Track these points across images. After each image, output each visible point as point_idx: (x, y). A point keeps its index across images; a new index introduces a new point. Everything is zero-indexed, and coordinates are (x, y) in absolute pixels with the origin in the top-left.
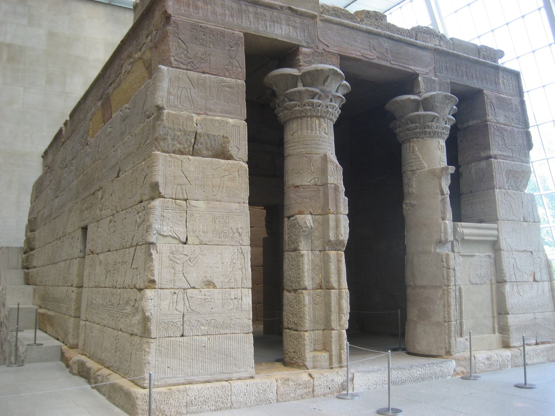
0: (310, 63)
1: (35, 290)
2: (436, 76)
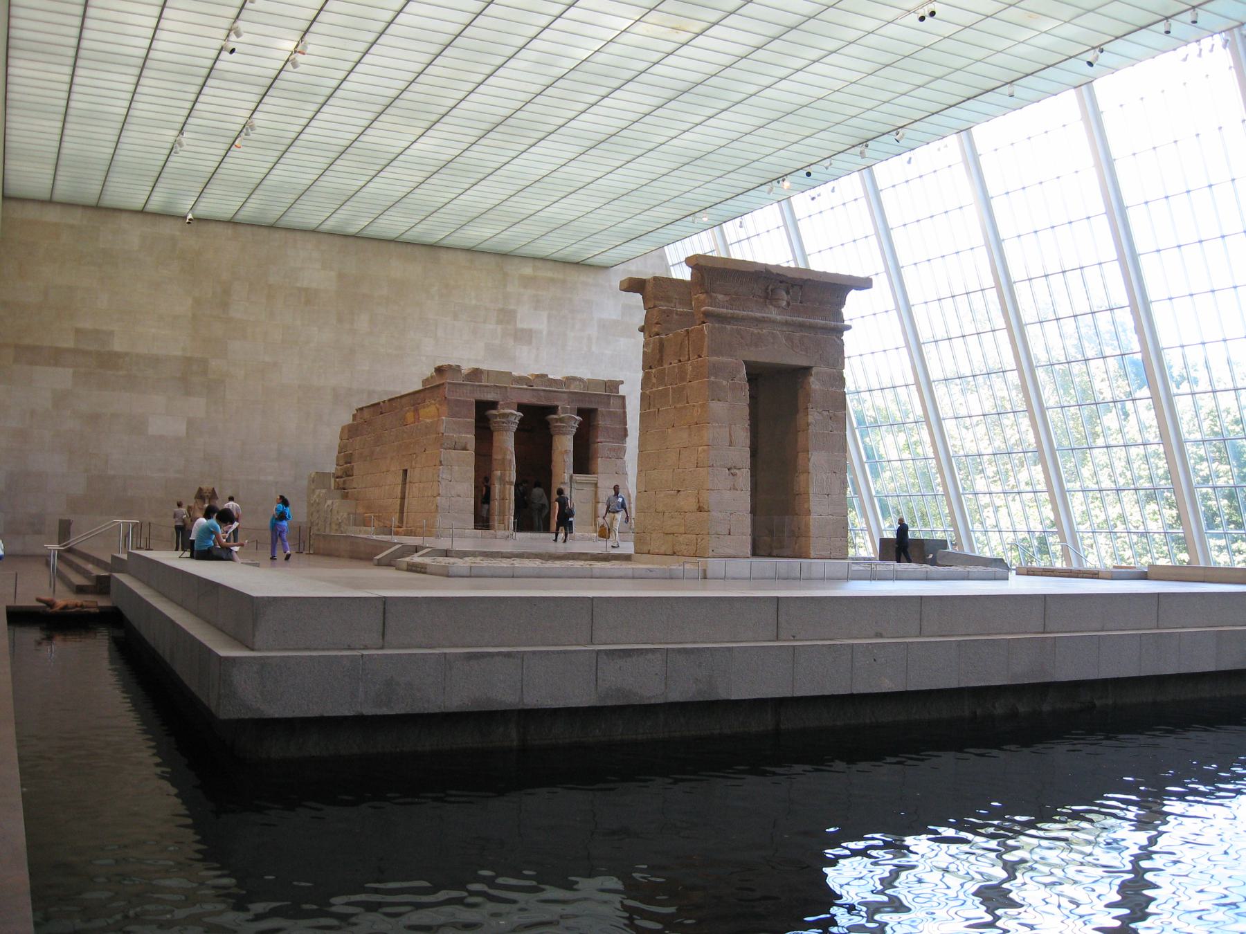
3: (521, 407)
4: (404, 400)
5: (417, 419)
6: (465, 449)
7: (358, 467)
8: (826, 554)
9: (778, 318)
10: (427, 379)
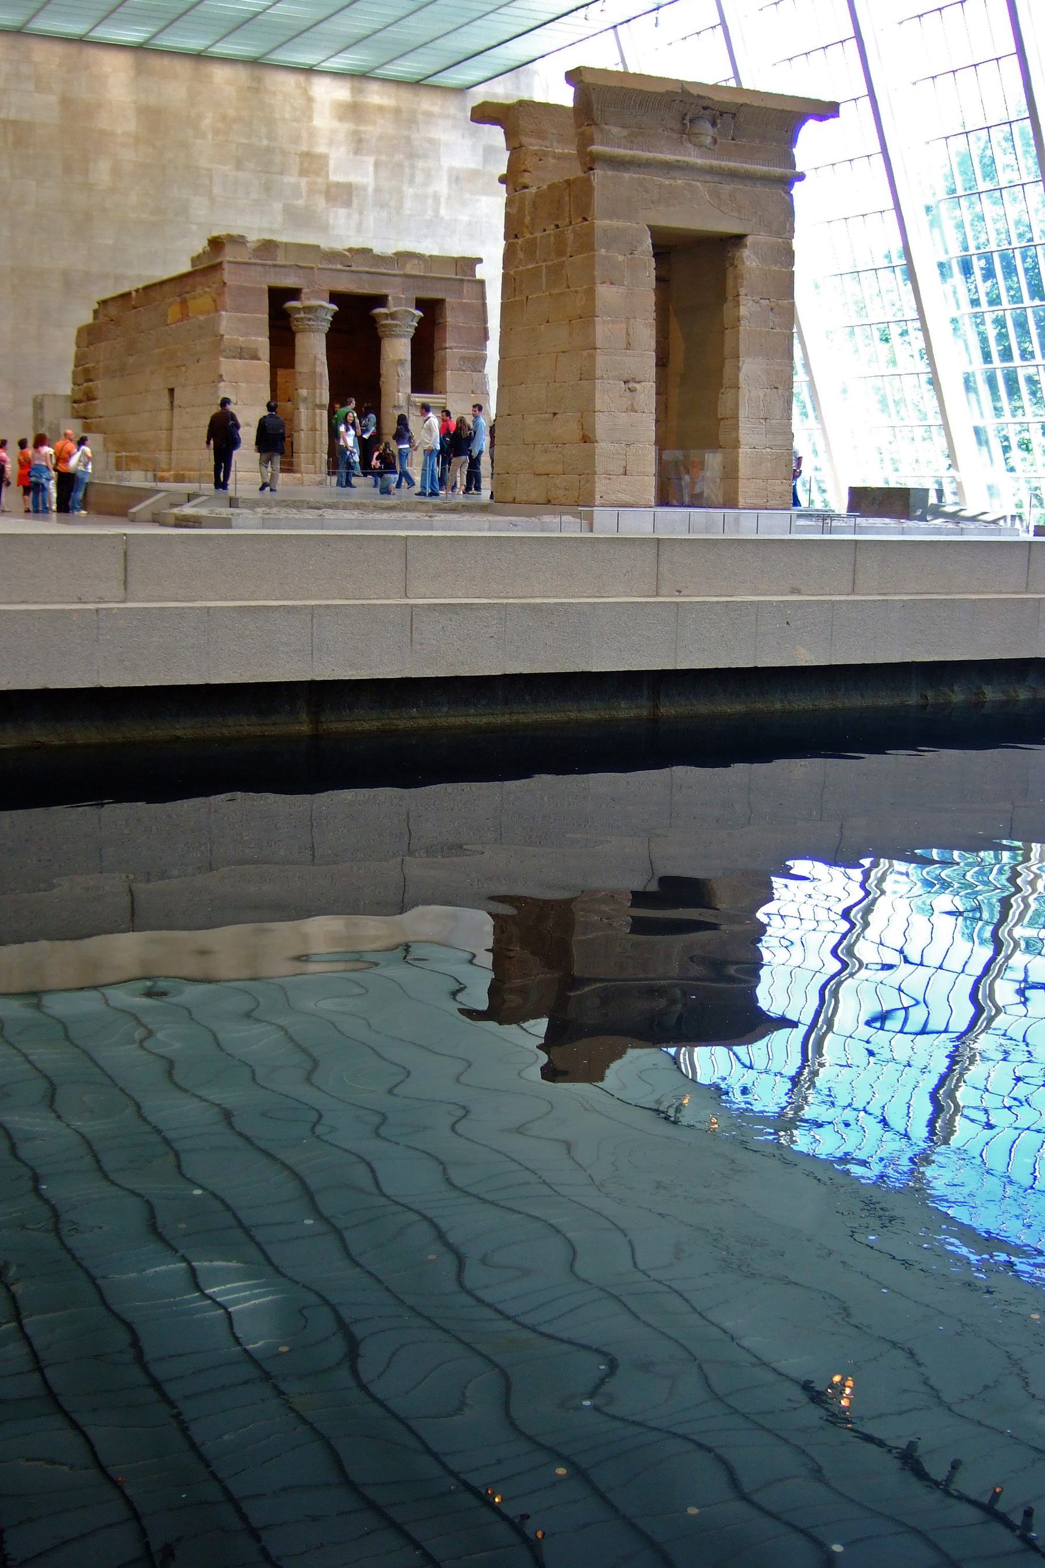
0: (309, 299)
1: (105, 439)
3: (335, 297)
4: (166, 289)
5: (185, 316)
6: (255, 357)
7: (100, 386)
8: (761, 502)
9: (699, 161)
10: (199, 257)
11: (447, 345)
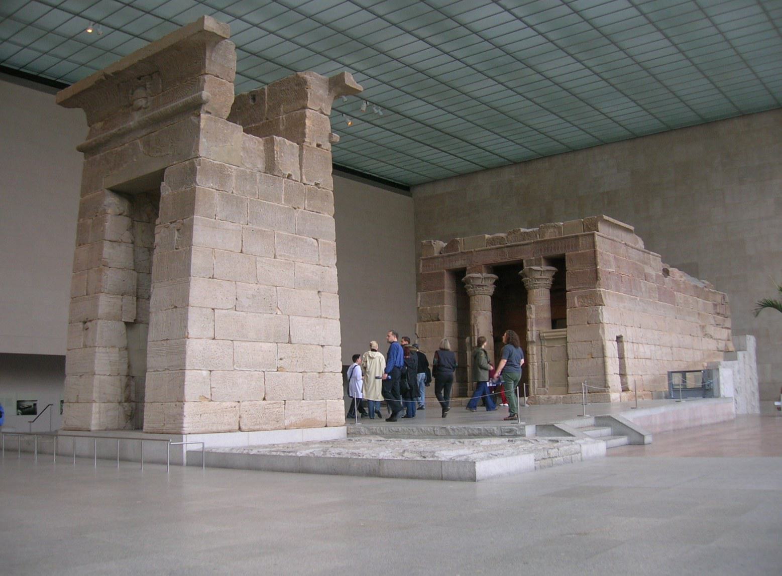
2: (533, 256)
11: (567, 289)
